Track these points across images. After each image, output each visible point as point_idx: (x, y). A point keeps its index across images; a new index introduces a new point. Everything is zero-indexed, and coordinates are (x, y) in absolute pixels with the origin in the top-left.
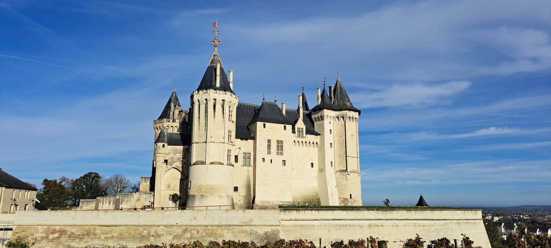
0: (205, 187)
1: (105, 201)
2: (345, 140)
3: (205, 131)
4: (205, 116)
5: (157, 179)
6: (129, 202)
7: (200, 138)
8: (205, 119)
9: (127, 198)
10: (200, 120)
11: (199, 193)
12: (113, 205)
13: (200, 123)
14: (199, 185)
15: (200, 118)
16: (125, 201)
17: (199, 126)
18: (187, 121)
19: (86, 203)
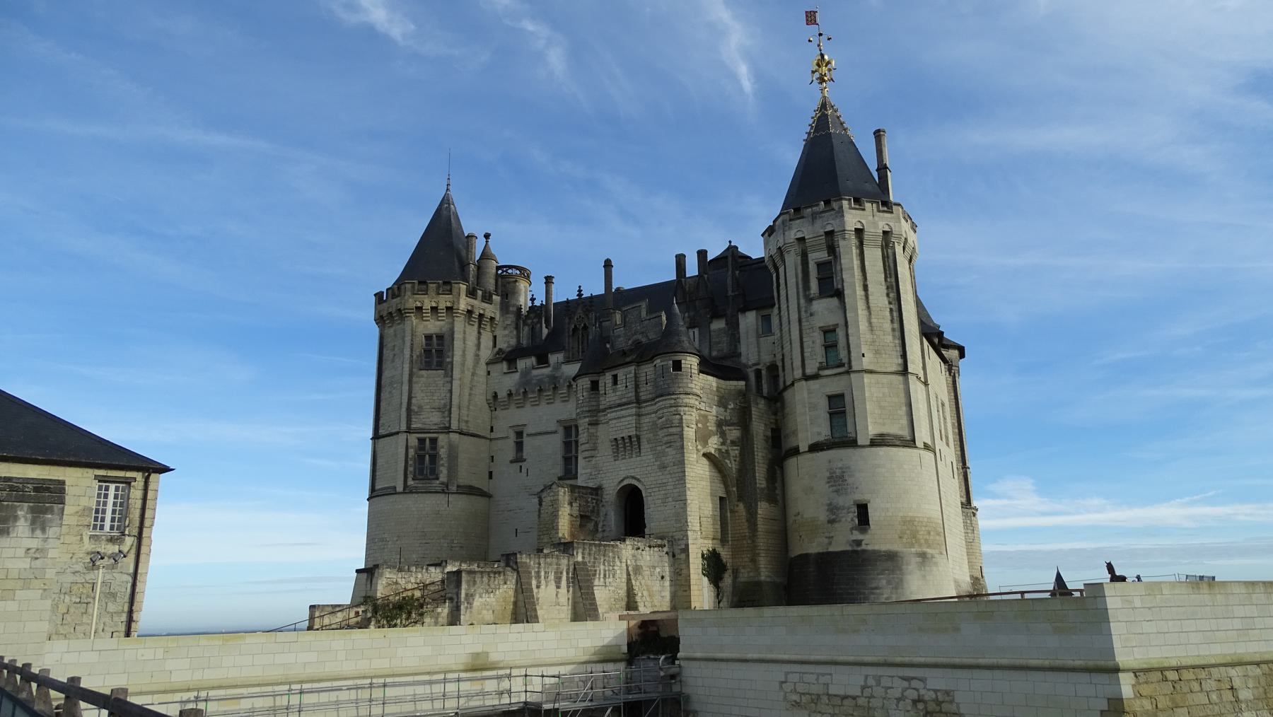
0: (924, 524)
1: (543, 574)
2: (956, 424)
3: (894, 337)
4: (888, 288)
5: (689, 488)
6: (611, 580)
7: (878, 356)
8: (888, 295)
9: (604, 564)
10: (870, 297)
11: (912, 545)
12: (568, 591)
13: (871, 305)
14: (908, 519)
15: (869, 289)
16: (600, 574)
17: (870, 314)
18: (544, 303)
19: (485, 579)
